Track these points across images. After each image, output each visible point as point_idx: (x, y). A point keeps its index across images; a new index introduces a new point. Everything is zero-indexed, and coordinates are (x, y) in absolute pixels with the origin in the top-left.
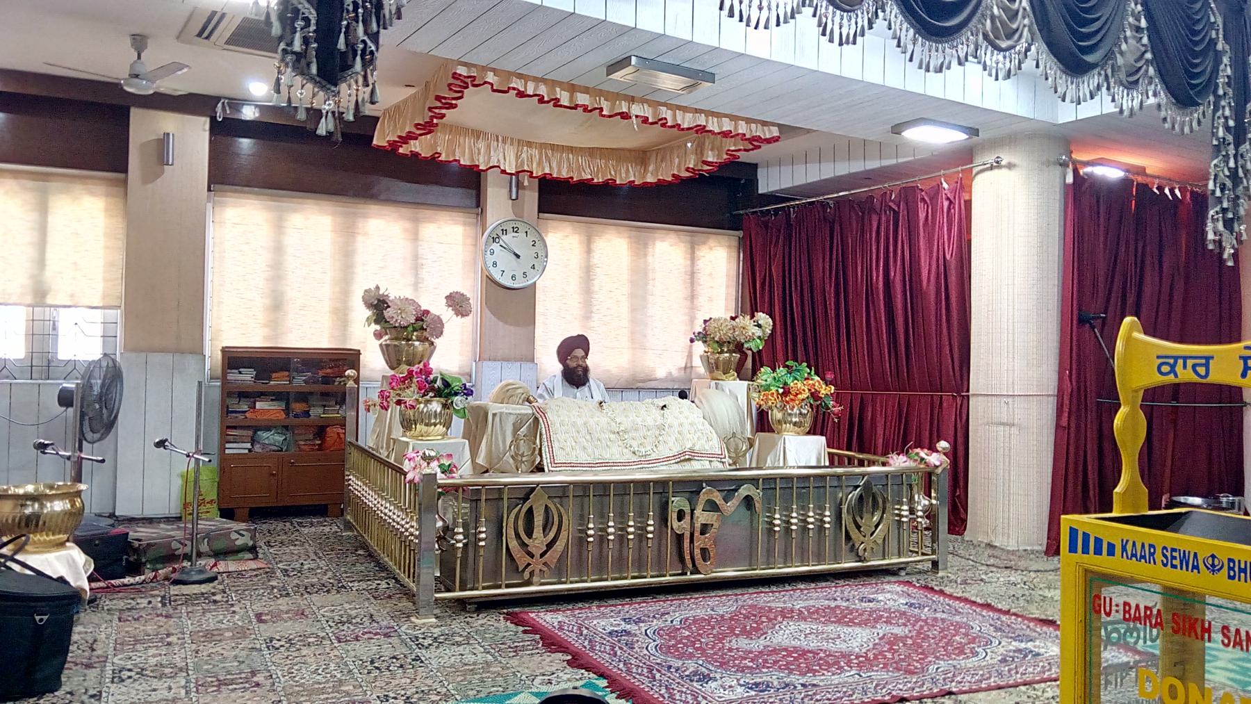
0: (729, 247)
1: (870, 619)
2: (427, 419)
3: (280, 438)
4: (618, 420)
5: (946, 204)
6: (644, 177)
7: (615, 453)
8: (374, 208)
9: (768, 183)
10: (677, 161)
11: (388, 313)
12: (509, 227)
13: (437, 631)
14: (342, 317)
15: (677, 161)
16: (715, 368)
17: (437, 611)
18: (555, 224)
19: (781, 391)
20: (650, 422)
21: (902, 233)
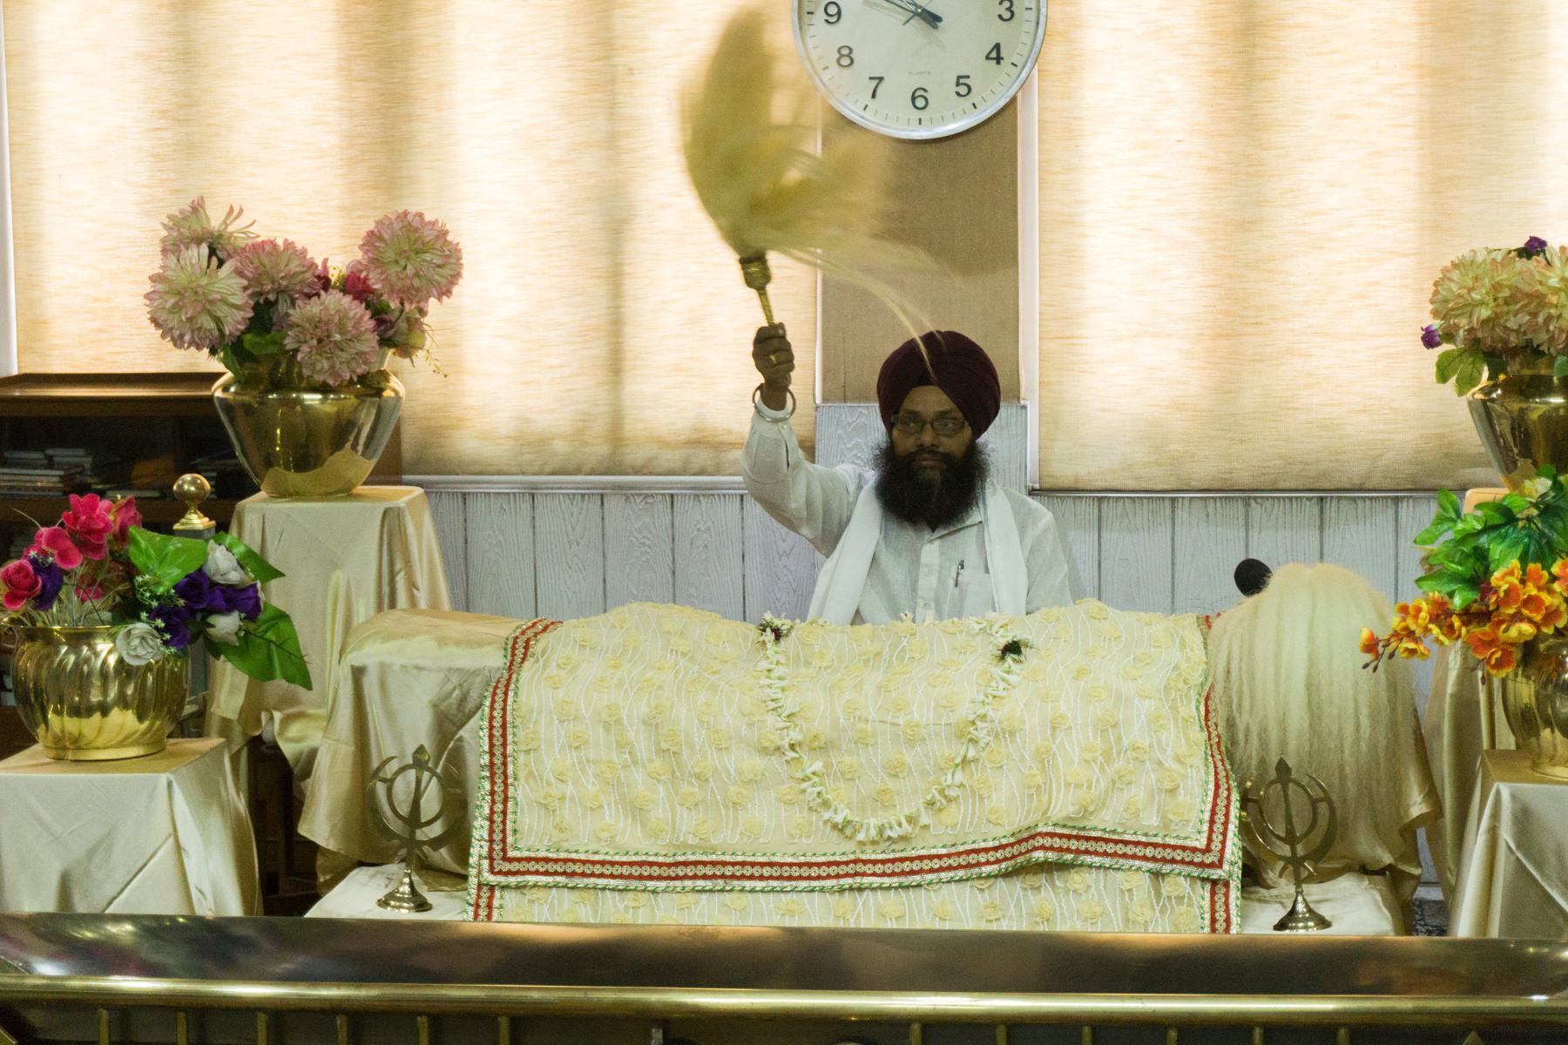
7: (772, 826)
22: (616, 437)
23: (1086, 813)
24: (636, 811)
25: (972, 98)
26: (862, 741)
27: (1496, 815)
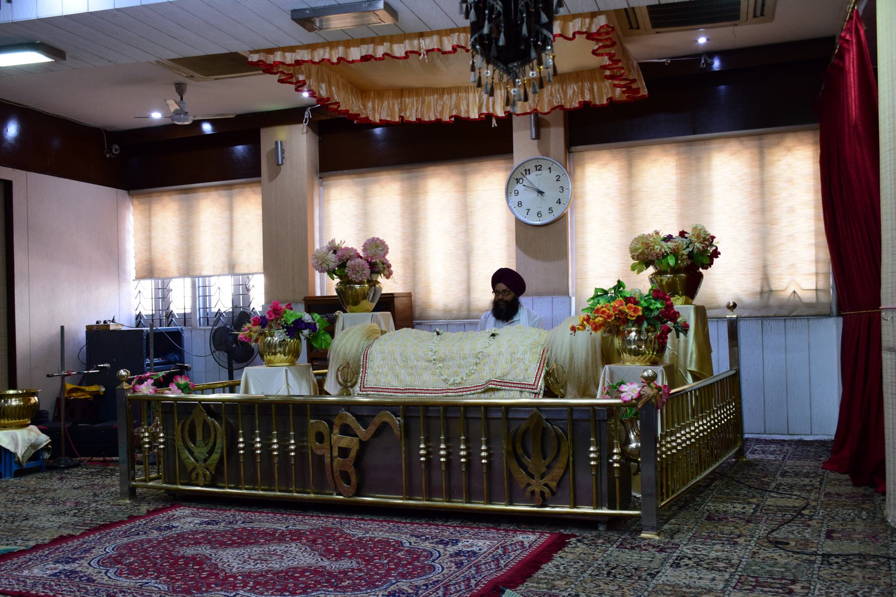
8: (431, 170)
12: (531, 166)
18: (588, 155)
22: (469, 309)
23: (504, 376)
26: (452, 359)
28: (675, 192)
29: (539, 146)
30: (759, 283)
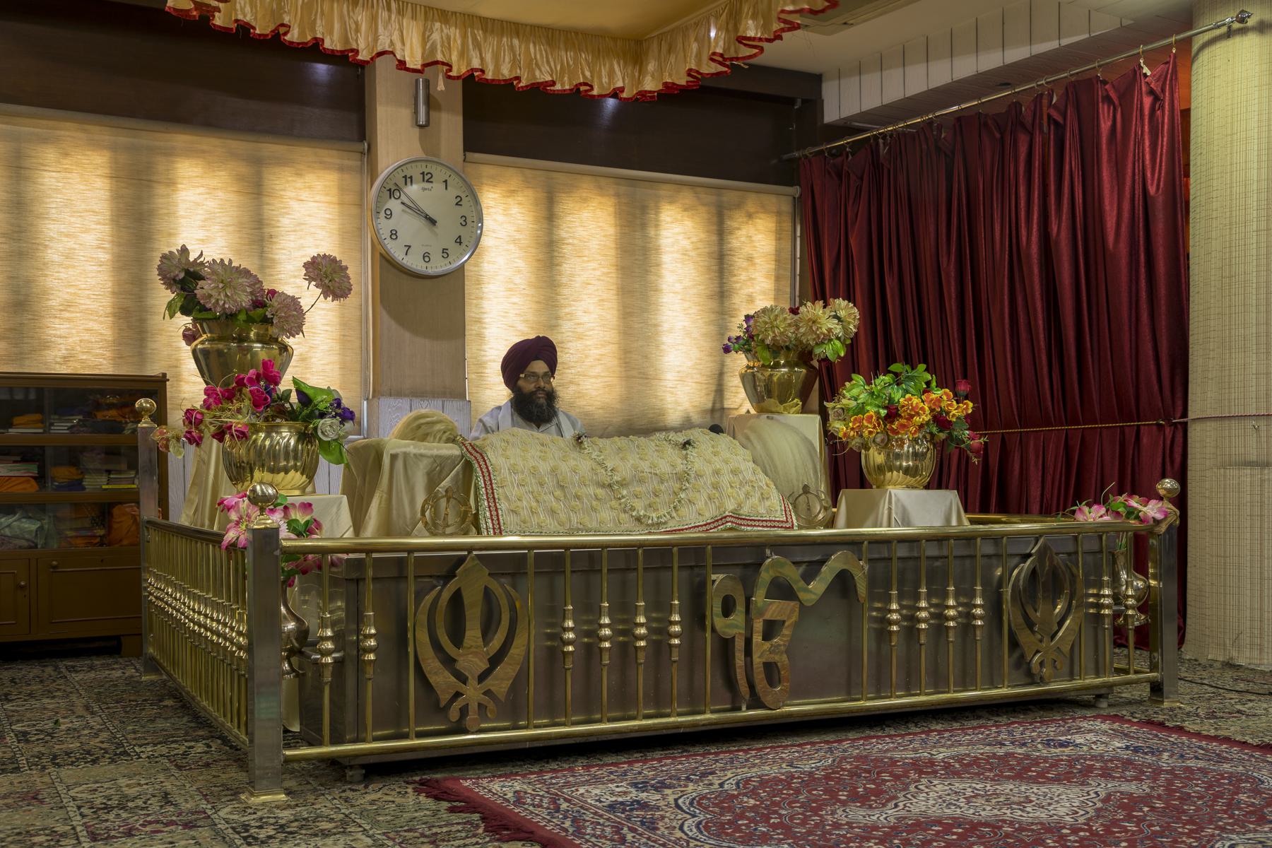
0: (779, 213)
1: (1076, 772)
2: (272, 461)
3: (30, 526)
4: (609, 465)
5: (1147, 101)
6: (640, 82)
9: (843, 102)
10: (695, 46)
11: (204, 289)
12: (415, 171)
13: (286, 815)
14: (132, 322)
15: (695, 46)
16: (765, 394)
17: (291, 784)
18: (487, 170)
19: (883, 412)
20: (664, 467)
21: (1072, 161)
24: (553, 512)
25: (450, 259)
27: (890, 502)
28: (613, 252)
29: (423, 140)
30: (711, 397)
